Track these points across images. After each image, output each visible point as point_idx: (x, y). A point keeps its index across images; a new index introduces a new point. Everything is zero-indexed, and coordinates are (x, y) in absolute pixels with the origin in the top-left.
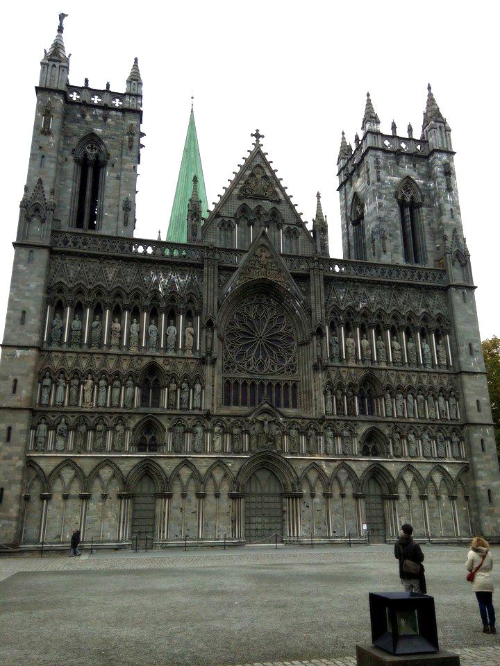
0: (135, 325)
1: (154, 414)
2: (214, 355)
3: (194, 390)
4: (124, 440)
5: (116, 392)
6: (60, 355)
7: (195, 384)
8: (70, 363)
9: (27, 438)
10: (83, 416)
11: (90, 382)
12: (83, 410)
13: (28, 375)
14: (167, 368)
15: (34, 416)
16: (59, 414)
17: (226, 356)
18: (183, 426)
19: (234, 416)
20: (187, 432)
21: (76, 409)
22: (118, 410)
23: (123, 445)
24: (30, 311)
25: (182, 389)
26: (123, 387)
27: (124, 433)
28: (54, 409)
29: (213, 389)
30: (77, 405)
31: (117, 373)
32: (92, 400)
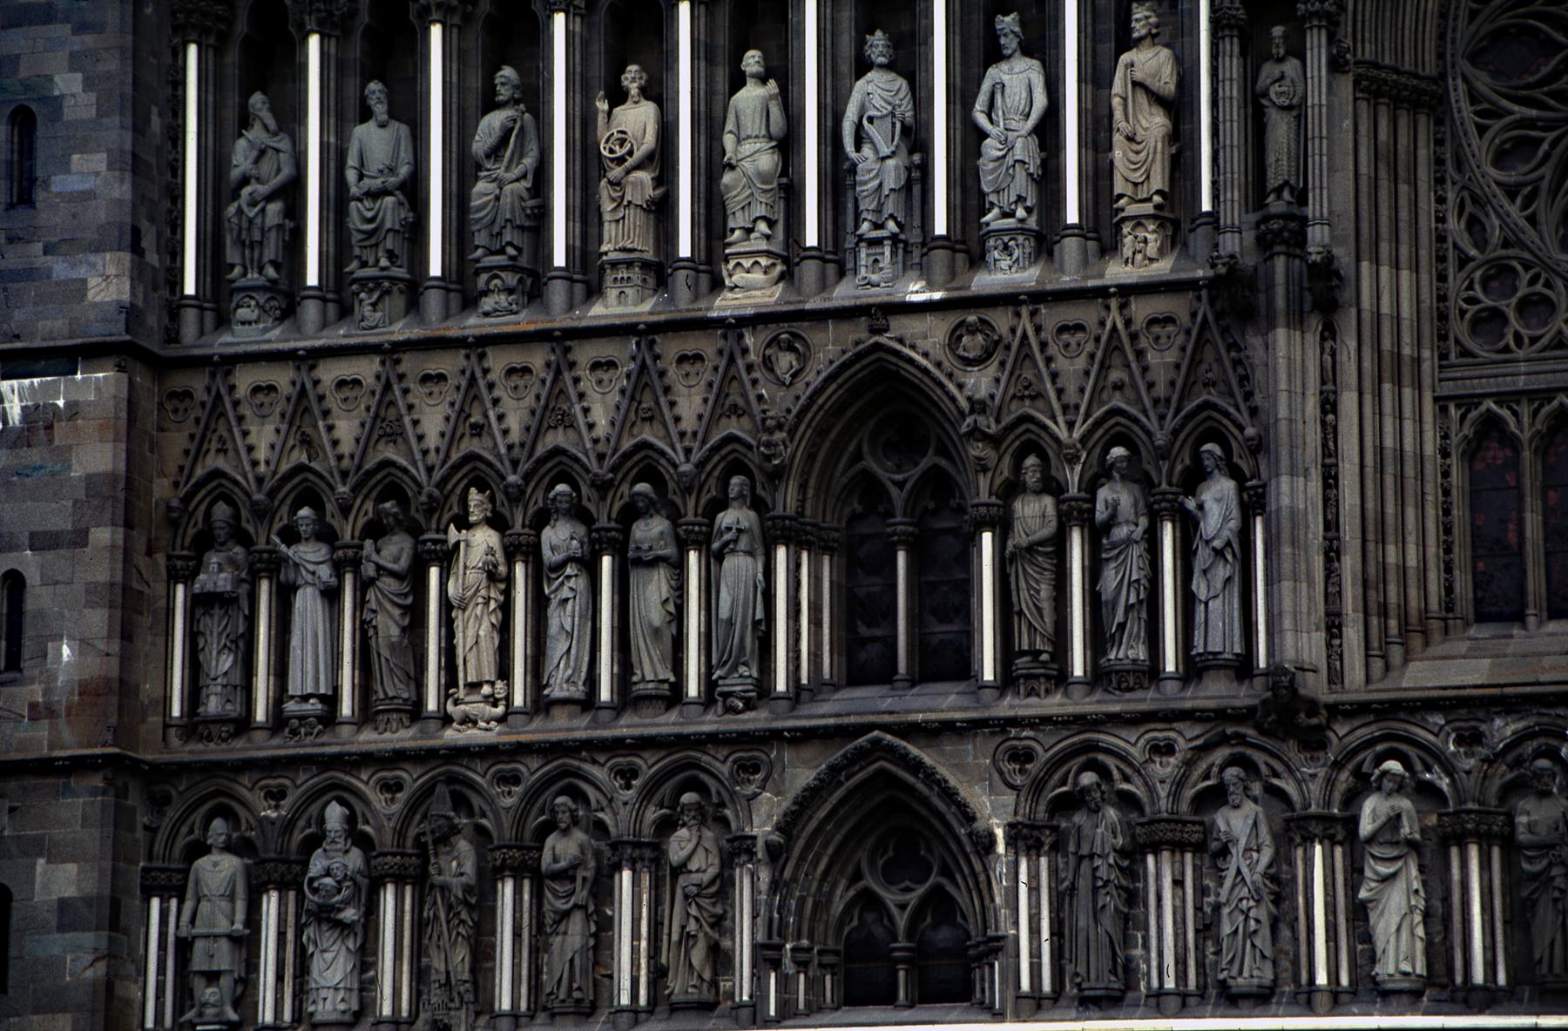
0: (751, 96)
1: (910, 731)
2: (1317, 235)
3: (1188, 527)
4: (721, 923)
5: (652, 590)
6: (282, 377)
7: (1195, 478)
8: (347, 429)
9: (111, 956)
10: (451, 779)
11: (482, 542)
12: (452, 735)
13: (79, 538)
14: (980, 382)
15: (159, 803)
16: (306, 781)
17: (1475, 225)
18: (1128, 801)
19: (1506, 704)
20: (1156, 850)
21: (403, 737)
22: (668, 723)
23: (721, 959)
24: (55, 104)
25: (1097, 535)
26: (693, 557)
27: (723, 887)
28: (278, 747)
29: (1330, 501)
30: (415, 711)
31: (645, 462)
32: (505, 672)
